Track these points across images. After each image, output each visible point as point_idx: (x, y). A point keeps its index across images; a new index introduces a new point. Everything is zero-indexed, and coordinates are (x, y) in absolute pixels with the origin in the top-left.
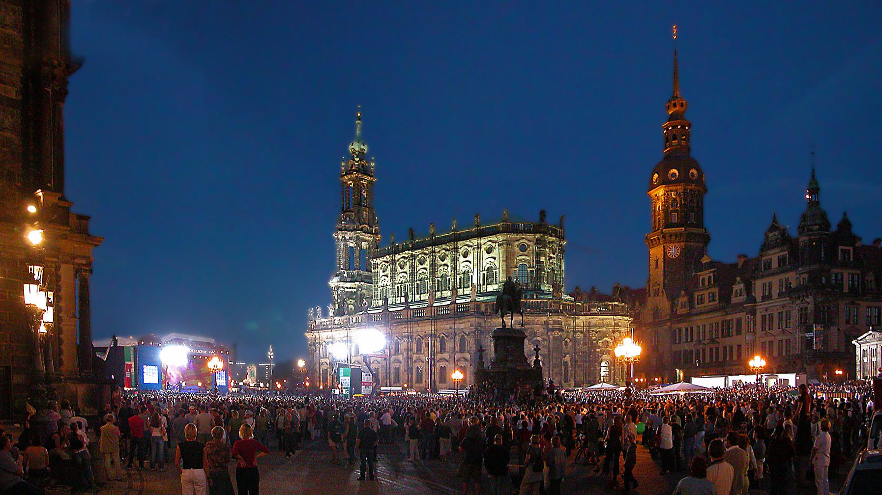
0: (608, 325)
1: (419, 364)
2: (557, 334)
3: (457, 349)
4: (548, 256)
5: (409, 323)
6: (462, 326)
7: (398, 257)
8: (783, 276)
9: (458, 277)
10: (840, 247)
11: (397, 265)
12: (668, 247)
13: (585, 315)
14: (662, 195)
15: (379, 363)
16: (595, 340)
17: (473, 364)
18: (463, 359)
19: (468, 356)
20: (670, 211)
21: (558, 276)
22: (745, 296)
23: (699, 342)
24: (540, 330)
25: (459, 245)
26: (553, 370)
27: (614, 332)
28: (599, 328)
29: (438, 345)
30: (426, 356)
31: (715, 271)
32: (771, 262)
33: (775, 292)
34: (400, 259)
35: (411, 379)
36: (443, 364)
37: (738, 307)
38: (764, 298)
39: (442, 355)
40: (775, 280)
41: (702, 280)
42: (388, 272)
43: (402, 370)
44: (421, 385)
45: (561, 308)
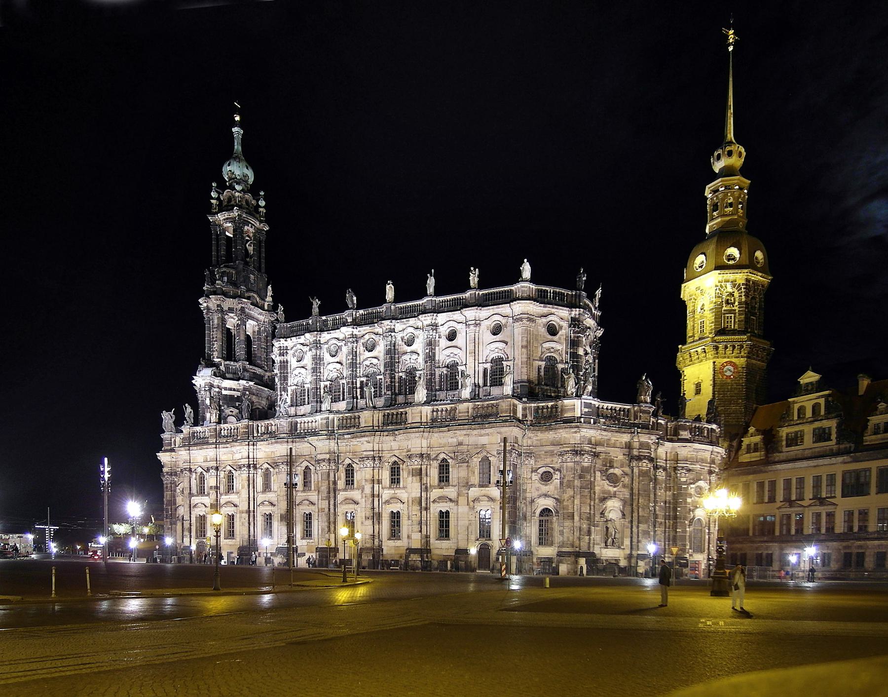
0: (703, 461)
1: (395, 507)
16: (685, 483)
26: (638, 527)
28: (691, 464)
36: (444, 507)
41: (799, 410)
44: (398, 543)
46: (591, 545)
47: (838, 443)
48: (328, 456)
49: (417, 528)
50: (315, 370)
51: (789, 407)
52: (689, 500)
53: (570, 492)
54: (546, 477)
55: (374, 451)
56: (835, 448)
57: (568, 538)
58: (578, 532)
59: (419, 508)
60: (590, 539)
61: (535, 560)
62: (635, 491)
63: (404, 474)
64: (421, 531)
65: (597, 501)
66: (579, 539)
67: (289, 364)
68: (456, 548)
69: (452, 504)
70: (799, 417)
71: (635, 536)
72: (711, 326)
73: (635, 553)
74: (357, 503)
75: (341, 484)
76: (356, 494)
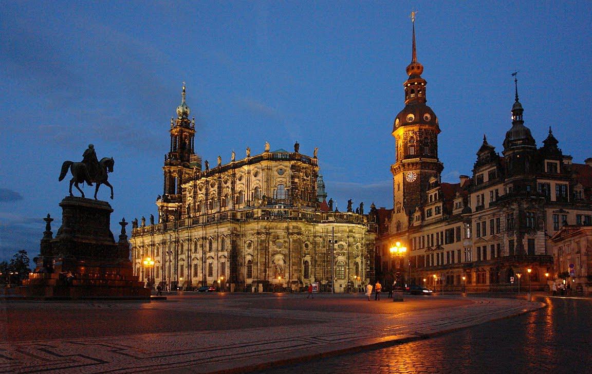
0: (343, 231)
1: (195, 262)
2: (296, 237)
3: (220, 248)
4: (302, 179)
6: (222, 230)
7: (198, 182)
8: (493, 188)
10: (546, 161)
11: (198, 188)
13: (324, 223)
17: (229, 260)
18: (223, 257)
19: (226, 254)
23: (429, 248)
24: (281, 233)
25: (236, 172)
27: (348, 237)
29: (208, 245)
30: (199, 255)
31: (439, 189)
32: (483, 177)
33: (487, 201)
34: (199, 184)
37: (458, 218)
38: (478, 209)
40: (487, 192)
42: (192, 194)
43: (184, 267)
45: (300, 216)
46: (267, 277)
47: (443, 215)
48: (174, 240)
52: (335, 252)
54: (249, 246)
56: (442, 217)
60: (265, 274)
62: (291, 250)
64: (203, 273)
65: (270, 255)
66: (260, 274)
71: (291, 272)
73: (291, 281)
74: (184, 260)
75: (179, 252)
76: (184, 257)
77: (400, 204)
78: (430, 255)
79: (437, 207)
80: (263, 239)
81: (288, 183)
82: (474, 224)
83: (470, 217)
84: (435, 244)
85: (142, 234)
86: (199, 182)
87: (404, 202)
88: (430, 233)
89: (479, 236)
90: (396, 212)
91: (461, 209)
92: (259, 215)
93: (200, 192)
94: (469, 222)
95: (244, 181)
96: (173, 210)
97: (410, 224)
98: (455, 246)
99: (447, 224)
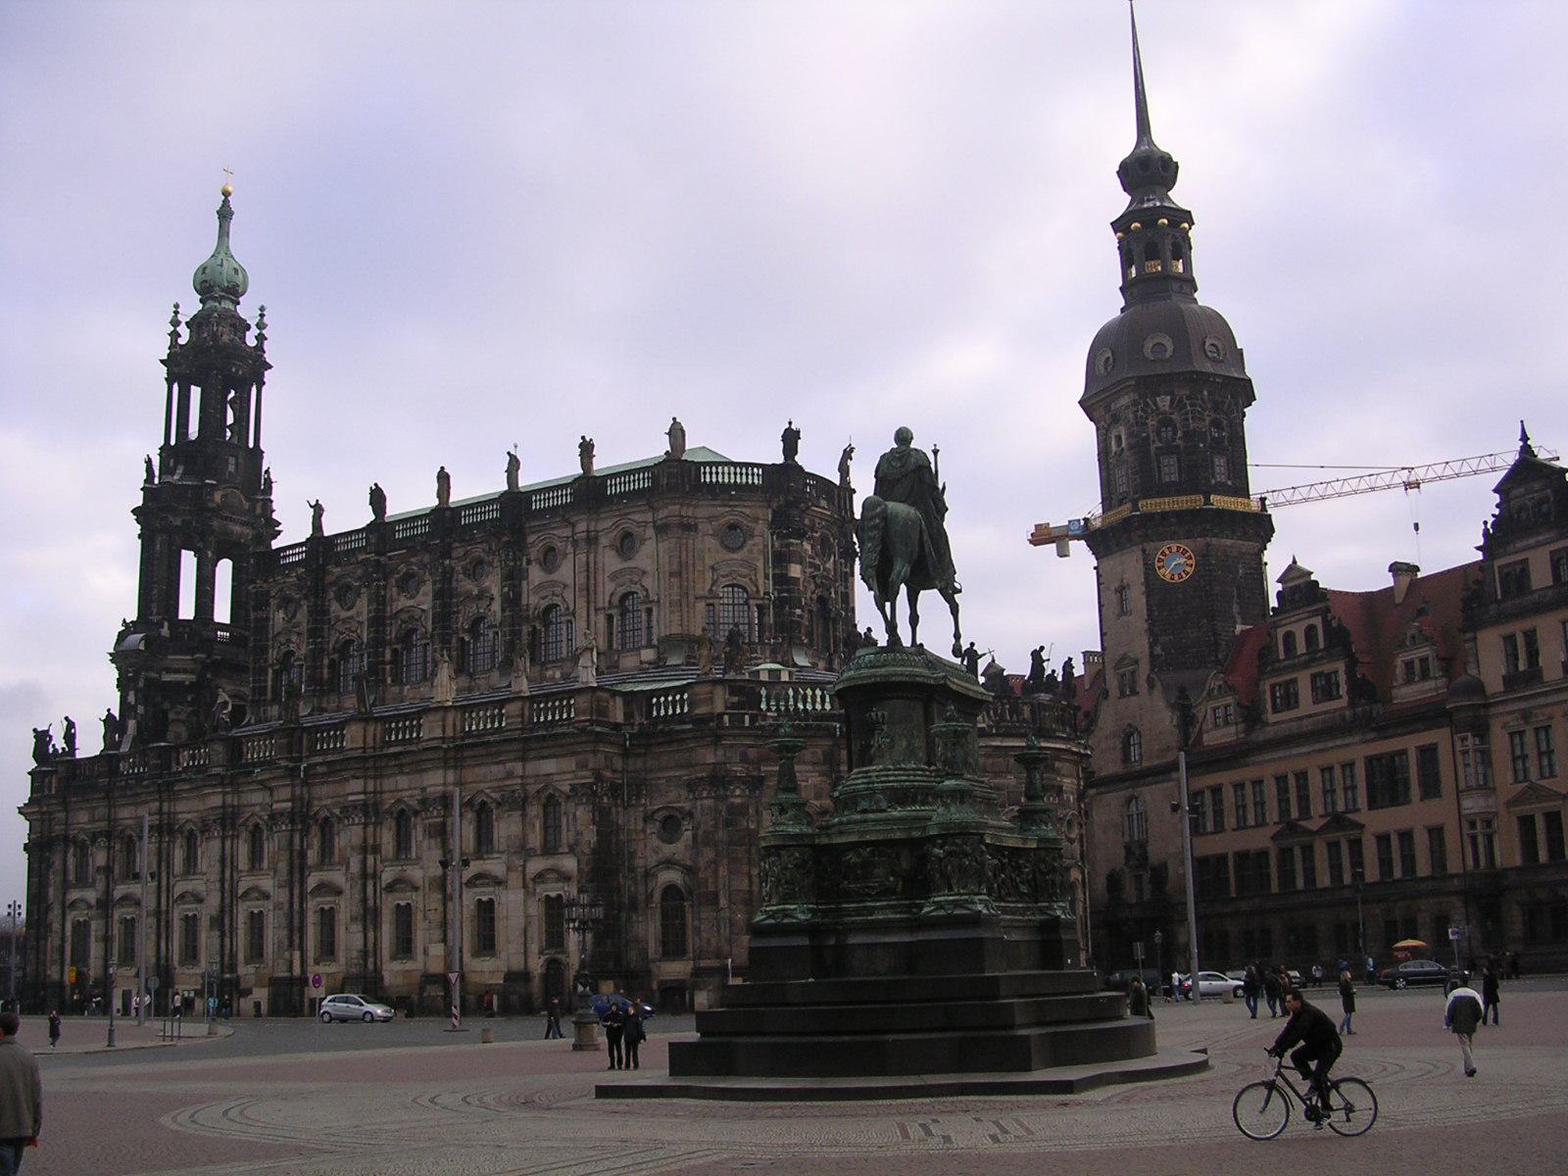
3: (535, 840)
5: (370, 764)
9: (526, 629)
12: (1158, 549)
14: (1127, 408)
15: (266, 896)
18: (553, 876)
19: (569, 864)
20: (1152, 452)
21: (840, 626)
22: (1441, 682)
35: (375, 944)
38: (1511, 681)
39: (482, 862)
42: (302, 617)
43: (342, 917)
44: (409, 965)
47: (1352, 704)
49: (437, 934)
50: (315, 633)
51: (1269, 634)
53: (709, 854)
54: (670, 826)
55: (365, 793)
57: (709, 940)
58: (728, 929)
59: (440, 896)
61: (655, 986)
63: (418, 834)
64: (444, 940)
66: (730, 942)
67: (271, 623)
68: (506, 970)
69: (499, 890)
70: (1287, 651)
72: (1135, 480)
74: (339, 892)
75: (312, 856)
77: (1136, 662)
78: (1297, 852)
79: (1321, 674)
80: (738, 801)
81: (761, 582)
82: (1499, 740)
83: (1482, 712)
84: (1317, 807)
85: (103, 781)
86: (338, 570)
87: (1153, 657)
88: (1282, 768)
89: (1526, 778)
90: (1114, 692)
91: (1429, 684)
92: (719, 708)
93: (344, 614)
94: (1481, 731)
95: (565, 571)
96: (184, 682)
97: (1186, 736)
98: (1414, 815)
99: (1372, 735)
